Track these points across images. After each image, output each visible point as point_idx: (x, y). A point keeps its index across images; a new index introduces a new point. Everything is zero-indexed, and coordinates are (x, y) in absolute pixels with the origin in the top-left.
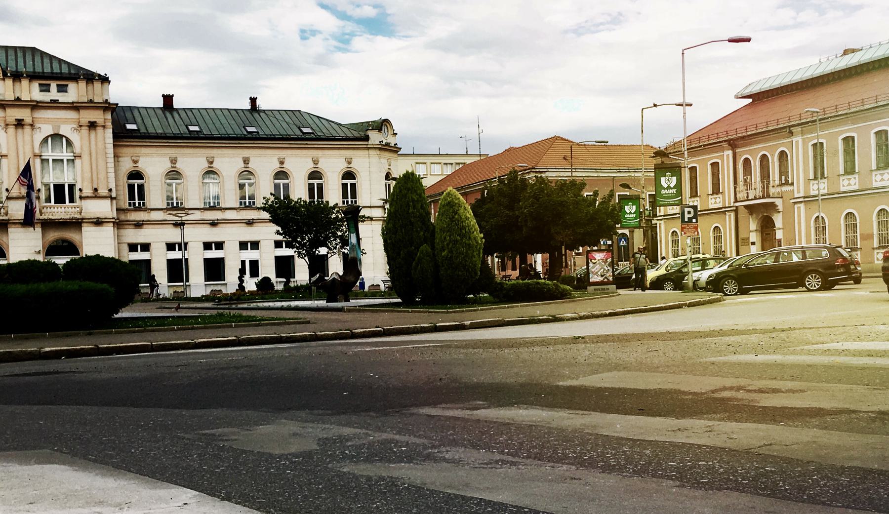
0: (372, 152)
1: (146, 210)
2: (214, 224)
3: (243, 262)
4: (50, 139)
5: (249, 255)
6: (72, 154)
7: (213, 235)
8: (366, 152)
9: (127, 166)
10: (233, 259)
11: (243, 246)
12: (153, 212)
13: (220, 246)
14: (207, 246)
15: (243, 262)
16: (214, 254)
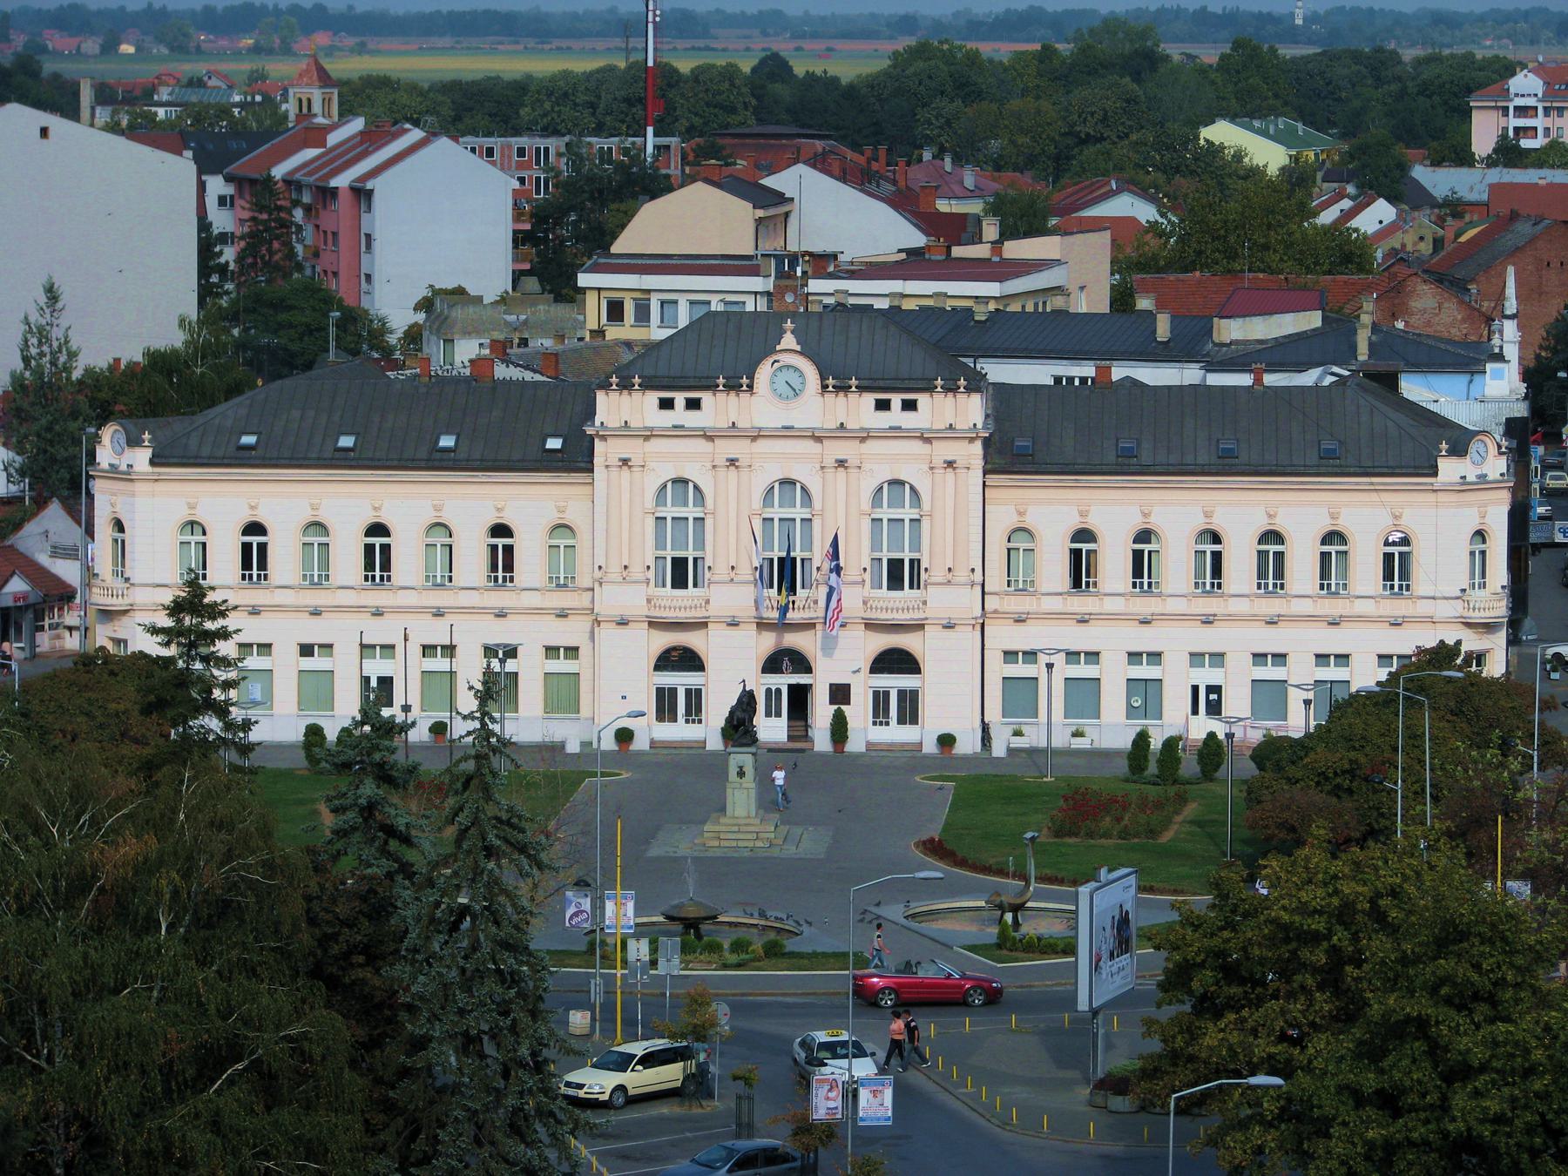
0: (1442, 497)
1: (1033, 594)
2: (1208, 621)
3: (1195, 689)
4: (886, 486)
5: (1206, 676)
6: (917, 510)
7: (1144, 640)
8: (1431, 497)
9: (1002, 518)
10: (1177, 681)
11: (1196, 658)
12: (1044, 598)
13: (1155, 657)
14: (1134, 657)
15: (1195, 689)
16: (1145, 671)
